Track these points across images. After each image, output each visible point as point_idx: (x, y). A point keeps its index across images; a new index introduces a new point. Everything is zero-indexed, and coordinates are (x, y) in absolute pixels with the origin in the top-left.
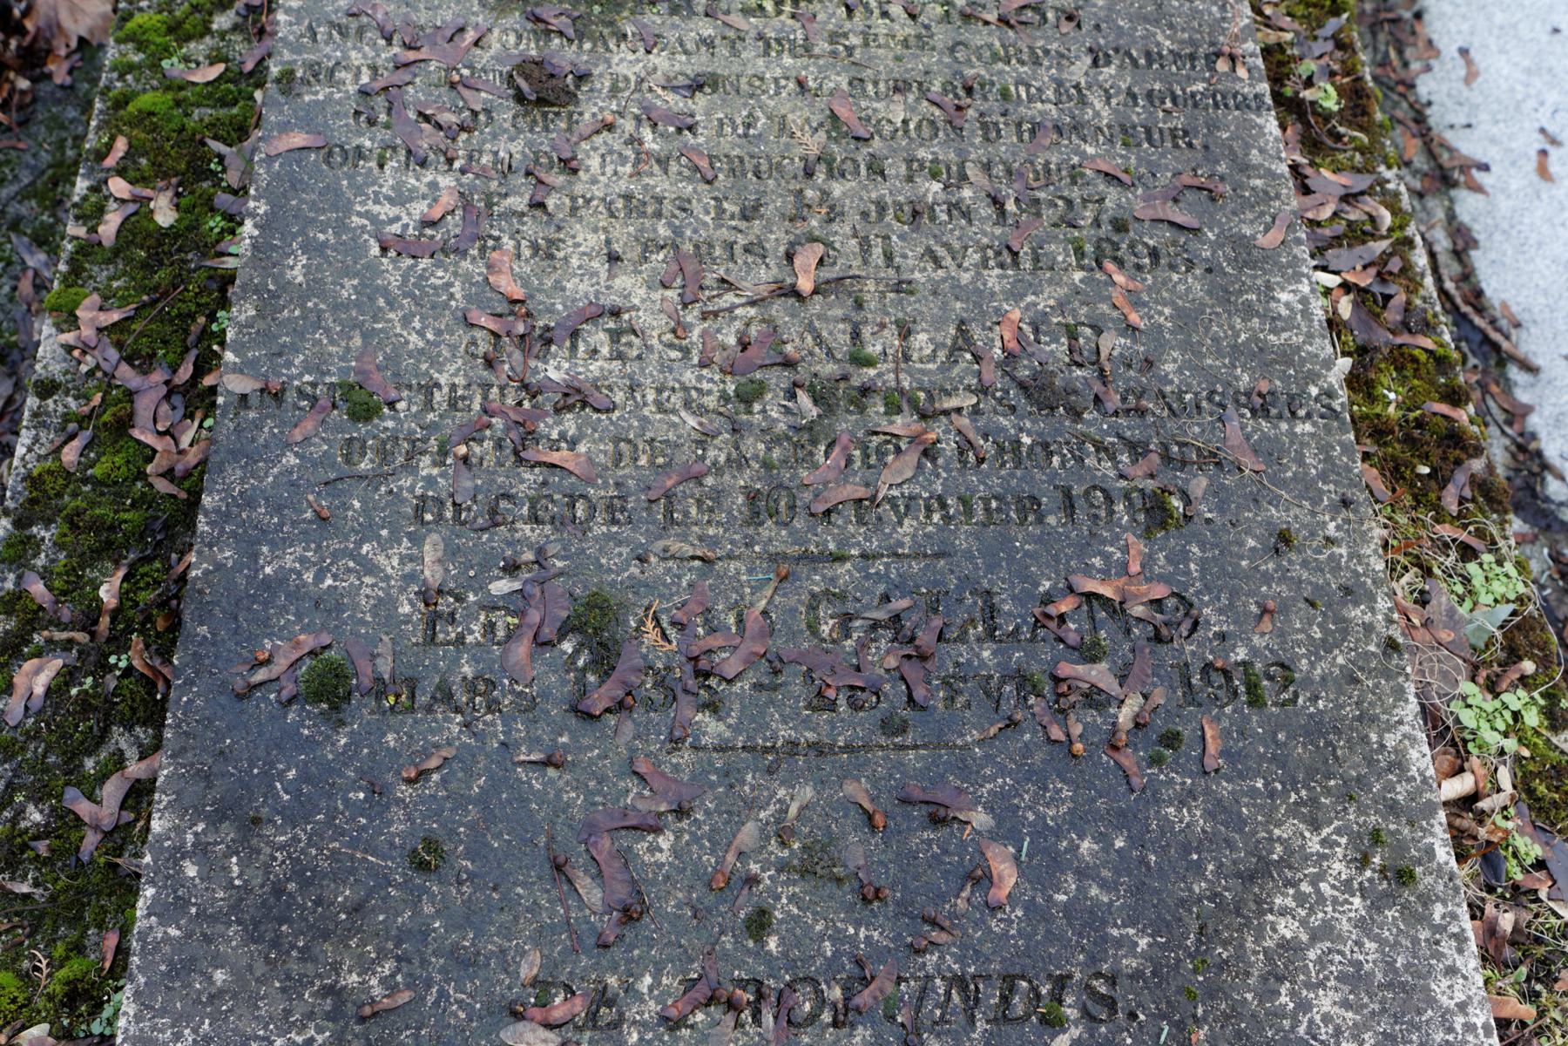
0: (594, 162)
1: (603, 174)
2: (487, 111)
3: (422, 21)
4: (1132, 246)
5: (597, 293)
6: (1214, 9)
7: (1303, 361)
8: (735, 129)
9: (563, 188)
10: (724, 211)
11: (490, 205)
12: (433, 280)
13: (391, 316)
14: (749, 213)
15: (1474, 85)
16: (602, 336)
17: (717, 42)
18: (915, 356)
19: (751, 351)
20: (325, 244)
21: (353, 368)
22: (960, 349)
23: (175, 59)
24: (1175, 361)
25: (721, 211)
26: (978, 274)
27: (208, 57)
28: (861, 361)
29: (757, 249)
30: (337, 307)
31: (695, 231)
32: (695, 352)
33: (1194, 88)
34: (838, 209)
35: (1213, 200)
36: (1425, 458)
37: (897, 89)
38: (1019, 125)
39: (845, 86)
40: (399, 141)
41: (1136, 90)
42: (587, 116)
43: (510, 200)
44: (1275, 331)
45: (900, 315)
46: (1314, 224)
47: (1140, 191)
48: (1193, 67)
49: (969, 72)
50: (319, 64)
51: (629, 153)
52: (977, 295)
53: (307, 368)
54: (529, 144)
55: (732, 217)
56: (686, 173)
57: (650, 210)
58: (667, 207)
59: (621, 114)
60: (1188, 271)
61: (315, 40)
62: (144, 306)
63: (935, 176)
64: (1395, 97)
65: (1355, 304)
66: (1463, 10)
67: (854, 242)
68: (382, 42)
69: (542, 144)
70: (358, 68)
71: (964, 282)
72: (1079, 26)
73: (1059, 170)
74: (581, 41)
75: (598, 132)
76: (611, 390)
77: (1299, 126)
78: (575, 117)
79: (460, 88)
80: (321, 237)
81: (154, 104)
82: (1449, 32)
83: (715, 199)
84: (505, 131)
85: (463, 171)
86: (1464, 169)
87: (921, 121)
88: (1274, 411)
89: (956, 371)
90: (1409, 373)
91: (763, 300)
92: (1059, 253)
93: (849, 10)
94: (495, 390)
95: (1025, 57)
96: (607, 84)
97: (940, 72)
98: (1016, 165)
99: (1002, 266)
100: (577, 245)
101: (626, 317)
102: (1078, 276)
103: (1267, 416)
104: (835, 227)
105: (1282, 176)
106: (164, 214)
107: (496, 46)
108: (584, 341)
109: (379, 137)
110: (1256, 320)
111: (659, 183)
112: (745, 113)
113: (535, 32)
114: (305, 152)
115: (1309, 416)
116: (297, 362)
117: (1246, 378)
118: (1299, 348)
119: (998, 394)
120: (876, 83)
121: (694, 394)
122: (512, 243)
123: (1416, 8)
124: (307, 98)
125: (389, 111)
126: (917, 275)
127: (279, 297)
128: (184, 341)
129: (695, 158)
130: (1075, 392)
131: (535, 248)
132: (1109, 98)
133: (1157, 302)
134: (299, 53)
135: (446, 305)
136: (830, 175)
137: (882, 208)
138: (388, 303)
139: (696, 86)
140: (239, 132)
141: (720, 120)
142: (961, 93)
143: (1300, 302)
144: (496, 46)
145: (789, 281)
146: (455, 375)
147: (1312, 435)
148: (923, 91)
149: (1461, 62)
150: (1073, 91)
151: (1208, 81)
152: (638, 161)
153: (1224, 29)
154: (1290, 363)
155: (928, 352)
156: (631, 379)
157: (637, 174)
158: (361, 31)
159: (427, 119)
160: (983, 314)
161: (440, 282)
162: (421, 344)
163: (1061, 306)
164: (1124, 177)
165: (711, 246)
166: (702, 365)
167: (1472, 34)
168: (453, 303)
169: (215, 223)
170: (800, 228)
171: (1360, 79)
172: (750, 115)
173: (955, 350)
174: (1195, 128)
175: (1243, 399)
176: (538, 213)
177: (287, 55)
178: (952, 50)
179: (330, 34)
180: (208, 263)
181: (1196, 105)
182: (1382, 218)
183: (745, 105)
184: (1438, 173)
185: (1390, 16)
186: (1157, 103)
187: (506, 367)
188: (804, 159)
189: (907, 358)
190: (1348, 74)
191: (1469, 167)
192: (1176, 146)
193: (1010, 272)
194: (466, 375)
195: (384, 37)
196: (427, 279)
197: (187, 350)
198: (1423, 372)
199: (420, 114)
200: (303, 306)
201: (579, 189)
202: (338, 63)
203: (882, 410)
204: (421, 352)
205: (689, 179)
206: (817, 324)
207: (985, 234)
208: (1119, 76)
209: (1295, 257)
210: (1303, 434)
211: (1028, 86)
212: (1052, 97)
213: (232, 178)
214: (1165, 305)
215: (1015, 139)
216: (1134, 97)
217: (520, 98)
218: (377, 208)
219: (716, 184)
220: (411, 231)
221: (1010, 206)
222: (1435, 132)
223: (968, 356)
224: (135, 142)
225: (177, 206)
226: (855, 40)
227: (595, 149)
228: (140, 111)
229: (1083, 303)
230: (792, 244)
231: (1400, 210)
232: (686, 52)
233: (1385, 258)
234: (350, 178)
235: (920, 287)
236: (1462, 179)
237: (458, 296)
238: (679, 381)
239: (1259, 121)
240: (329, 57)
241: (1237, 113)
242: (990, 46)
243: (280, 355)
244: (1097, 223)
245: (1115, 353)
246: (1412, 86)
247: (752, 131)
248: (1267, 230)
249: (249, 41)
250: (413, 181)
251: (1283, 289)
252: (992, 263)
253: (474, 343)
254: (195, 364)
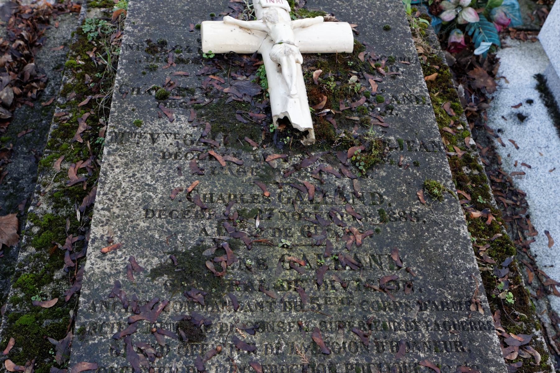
2: (168, 346)
6: (467, 278)
8: (272, 350)
15: (552, 248)
17: (264, 305)
23: (37, 296)
27: (51, 293)
33: (462, 320)
37: (340, 327)
38: (391, 343)
39: (318, 326)
40: (129, 364)
41: (438, 322)
42: (210, 346)
48: (461, 308)
49: (370, 316)
50: (96, 323)
51: (228, 366)
54: (185, 363)
59: (224, 345)
61: (94, 310)
64: (522, 254)
66: (545, 214)
68: (123, 310)
69: (190, 362)
70: (113, 324)
72: (413, 290)
73: (410, 366)
74: (207, 305)
75: (215, 355)
77: (499, 311)
79: (156, 334)
81: (27, 321)
82: (540, 224)
84: (175, 356)
86: (552, 286)
95: (392, 307)
96: (218, 329)
97: (357, 316)
98: (392, 365)
105: (502, 364)
107: (172, 310)
112: (276, 342)
113: (188, 302)
120: (331, 323)
123: (527, 213)
124: (90, 342)
129: (256, 367)
132: (428, 326)
134: (88, 318)
139: (254, 329)
140: (60, 333)
141: (266, 345)
142: (367, 327)
144: (172, 310)
148: (351, 327)
149: (546, 237)
150: (413, 324)
151: (467, 316)
153: (472, 289)
158: (115, 305)
159: (142, 351)
167: (549, 225)
171: (521, 287)
172: (279, 343)
174: (464, 341)
177: (83, 320)
178: (362, 304)
179: (102, 307)
181: (463, 329)
182: (537, 357)
183: (277, 337)
184: (542, 288)
185: (517, 217)
188: (302, 365)
190: (517, 285)
191: (554, 285)
192: (457, 351)
195: (124, 308)
199: (139, 349)
202: (104, 323)
208: (431, 315)
211: (394, 322)
212: (404, 328)
213: (58, 359)
215: (390, 350)
216: (438, 325)
217: (181, 339)
222: (539, 269)
224: (18, 341)
226: (321, 301)
227: (213, 364)
228: (21, 324)
231: (544, 352)
232: (251, 310)
236: (552, 290)
239: (490, 336)
240: (100, 319)
241: (481, 332)
242: (377, 302)
246: (529, 248)
247: (280, 351)
249: (69, 285)
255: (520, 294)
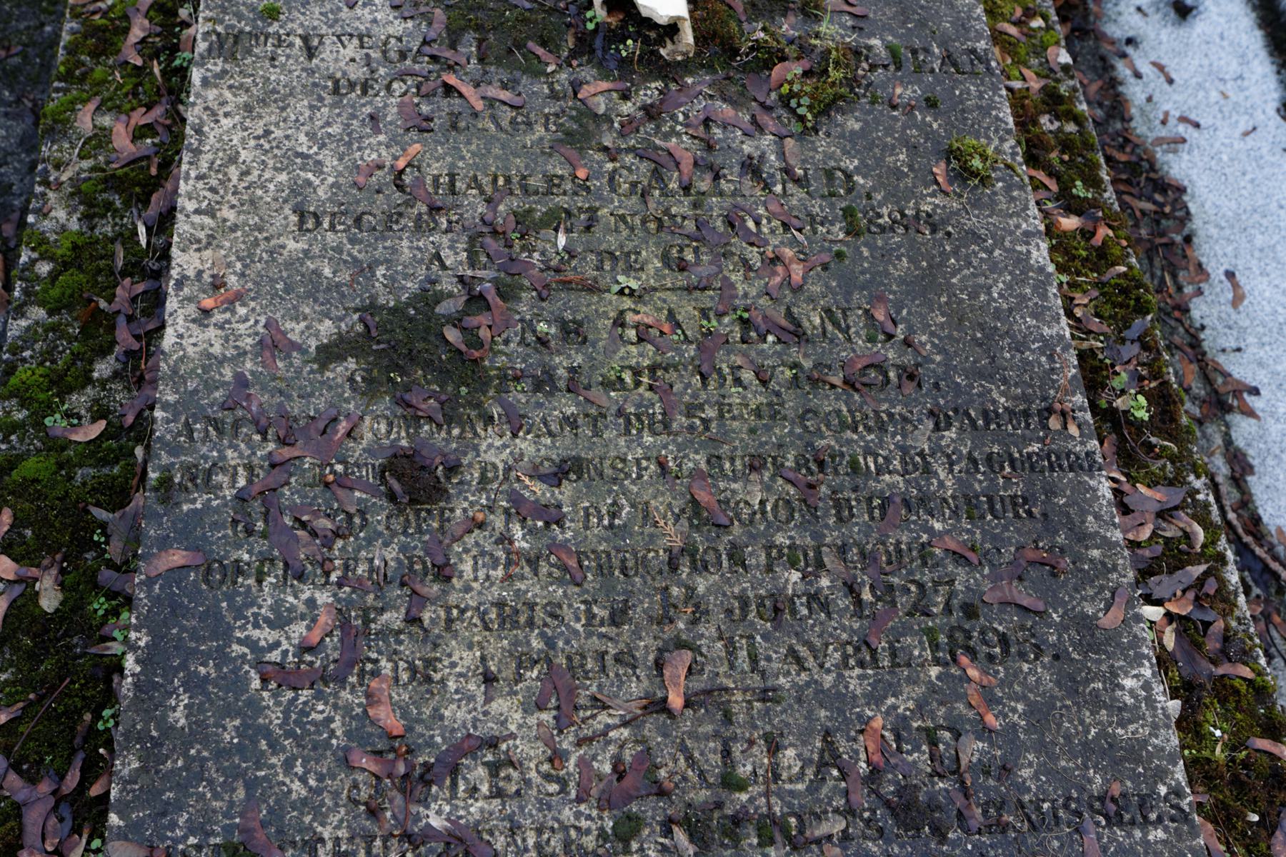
0: (467, 567)
1: (476, 579)
2: (362, 513)
3: (296, 411)
4: (982, 633)
5: (475, 720)
6: (1043, 359)
7: (1151, 756)
8: (601, 519)
9: (438, 598)
10: (594, 616)
11: (367, 621)
12: (314, 716)
13: (274, 760)
14: (618, 617)
15: (1241, 308)
16: (481, 771)
17: (580, 421)
18: (785, 776)
19: (627, 782)
20: (207, 677)
21: (238, 825)
22: (827, 764)
23: (58, 416)
24: (1030, 765)
25: (591, 616)
26: (840, 676)
27: (89, 410)
28: (731, 783)
29: (627, 658)
30: (221, 753)
31: (567, 642)
32: (572, 784)
33: (1030, 449)
34: (703, 607)
35: (1054, 575)
36: (1254, 805)
37: (752, 468)
38: (869, 500)
39: (703, 466)
40: (276, 553)
41: (976, 454)
42: (458, 512)
43: (386, 616)
44: (1122, 724)
45: (768, 728)
46: (1134, 545)
47: (986, 571)
48: (1028, 425)
49: (821, 443)
50: (196, 466)
51: (501, 554)
52: (838, 700)
53: (192, 831)
54: (403, 548)
55: (602, 624)
56: (556, 573)
57: (522, 619)
58: (540, 614)
59: (491, 509)
60: (1036, 658)
61: (191, 438)
62: (31, 704)
63: (793, 564)
64: (1173, 323)
65: (1178, 633)
66: (1227, 232)
67: (719, 645)
68: (257, 437)
69: (415, 548)
70: (235, 468)
71: (827, 686)
72: (919, 386)
73: (910, 550)
74: (449, 427)
75: (470, 531)
76: (492, 834)
77: (1114, 436)
78: (447, 513)
79: (334, 487)
80: (202, 670)
81: (38, 470)
82: (1215, 255)
83: (583, 602)
84: (380, 534)
85: (340, 585)
86: (1237, 393)
87: (777, 501)
88: (1127, 817)
89: (825, 791)
90: (1231, 706)
91: (635, 718)
92: (918, 649)
93: (704, 378)
94: (378, 843)
95: (871, 423)
96: (476, 475)
97: (792, 443)
98: (869, 547)
99: (861, 664)
100: (453, 665)
101: (504, 747)
102: (934, 671)
103: (1120, 823)
104: (701, 629)
105: (1117, 544)
106: (49, 600)
107: (369, 436)
108: (465, 778)
109: (257, 549)
110: (1104, 712)
111: (531, 587)
112: (609, 501)
113: (404, 417)
114: (184, 571)
115: (1160, 819)
116: (181, 821)
117: (1099, 780)
118: (1145, 743)
119: (866, 815)
120: (732, 460)
121: (573, 833)
122: (389, 665)
123: (1186, 232)
124: (185, 508)
125: (266, 516)
126: (782, 680)
127: (162, 745)
128: (71, 742)
129: (564, 556)
130: (939, 808)
131: (412, 669)
132: (951, 464)
133: (1010, 699)
134: (176, 455)
135: (327, 744)
136: (694, 568)
137: (745, 604)
138: (270, 745)
139: (560, 473)
140: (118, 496)
141: (586, 509)
142: (814, 467)
143: (1143, 688)
144: (369, 436)
145: (660, 694)
146: (338, 827)
147: (1164, 842)
148: (778, 467)
149: (1228, 284)
150: (918, 459)
151: (1042, 440)
152: (509, 563)
153: (1054, 381)
154: (1138, 761)
155: (796, 769)
156: (511, 821)
157: (508, 577)
158: (236, 425)
159: (303, 525)
160: (847, 721)
161: (320, 717)
162: (304, 793)
163: (921, 707)
164: (969, 555)
165: (583, 657)
166: (579, 800)
167: (1236, 257)
168: (334, 741)
169: (99, 605)
170: (668, 632)
171: (1166, 384)
172: (615, 503)
173: (822, 766)
174: (1033, 495)
175: (1097, 805)
176: (414, 629)
177: (165, 459)
178: (802, 418)
179: (207, 431)
180: (93, 650)
181: (1032, 468)
182: (1195, 534)
183: (610, 492)
184: (1214, 399)
185: (1164, 240)
186: (997, 468)
187: (388, 814)
188: (669, 550)
189: (777, 777)
190: (1156, 379)
191: (1241, 392)
192: (1017, 516)
193: (870, 672)
194: (348, 827)
195: (259, 432)
196: (308, 715)
197: (73, 752)
198: (1244, 704)
199: (297, 520)
200: (186, 755)
201: (453, 598)
202: (214, 465)
203: (755, 841)
204: (304, 802)
205: (560, 582)
206: (689, 743)
207: (844, 629)
208: (960, 440)
209: (1135, 636)
210: (1156, 842)
211: (876, 456)
212: (899, 468)
213: (114, 550)
214: (1017, 701)
215: (866, 517)
216: (974, 462)
217: (392, 497)
218: (256, 633)
219: (586, 586)
220: (290, 658)
221: (867, 596)
222: (1209, 356)
223: (835, 773)
224: (20, 515)
225: (62, 584)
226: (710, 413)
227: (466, 551)
228: (24, 478)
229: (942, 703)
230: (660, 651)
231: (1211, 523)
232: (551, 434)
233: (1201, 581)
234: (230, 598)
235: (786, 694)
236: (1235, 403)
237: (339, 733)
238: (557, 820)
239: (1091, 483)
240: (205, 458)
241: (1071, 475)
242: (838, 412)
243: (164, 814)
244: (948, 609)
245: (974, 760)
246: (1188, 311)
247: (617, 522)
248: (1107, 609)
249: (130, 391)
250: (291, 599)
251: (1126, 674)
252: (852, 662)
253: (355, 786)
254: (81, 771)
255: (1164, 401)
